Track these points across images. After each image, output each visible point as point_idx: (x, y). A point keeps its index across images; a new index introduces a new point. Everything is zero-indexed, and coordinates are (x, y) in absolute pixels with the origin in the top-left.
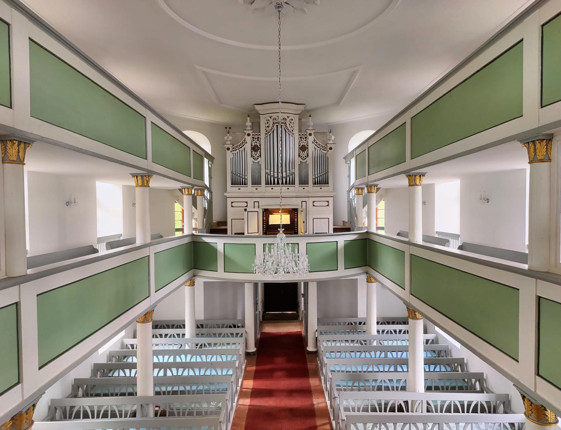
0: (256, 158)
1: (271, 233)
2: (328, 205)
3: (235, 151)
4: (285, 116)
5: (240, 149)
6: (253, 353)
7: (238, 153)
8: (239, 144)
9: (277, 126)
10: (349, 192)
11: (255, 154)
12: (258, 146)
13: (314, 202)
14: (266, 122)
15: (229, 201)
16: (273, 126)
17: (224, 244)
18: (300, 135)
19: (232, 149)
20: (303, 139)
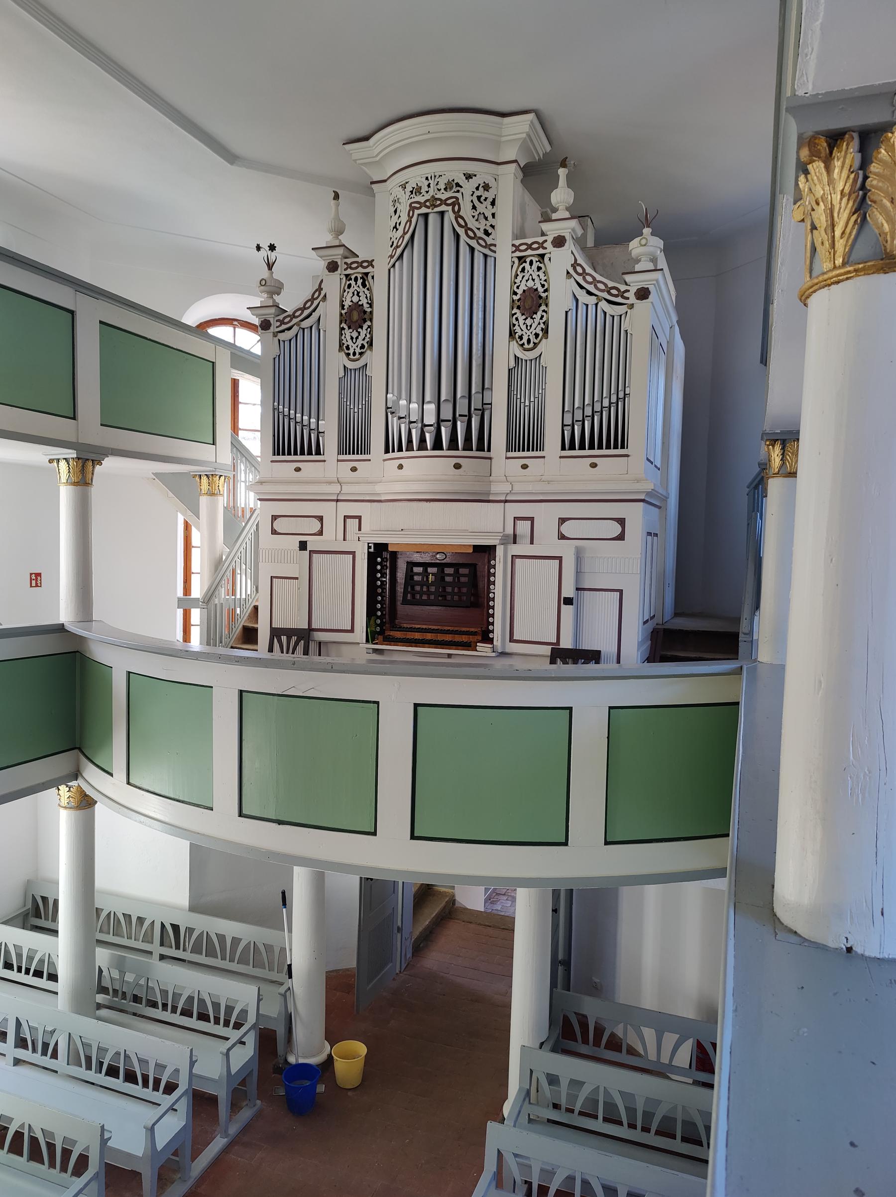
0: (354, 354)
1: (398, 634)
2: (621, 537)
4: (455, 171)
9: (426, 216)
11: (352, 338)
12: (362, 305)
13: (562, 521)
16: (410, 221)
18: (517, 248)
19: (278, 324)
20: (531, 263)
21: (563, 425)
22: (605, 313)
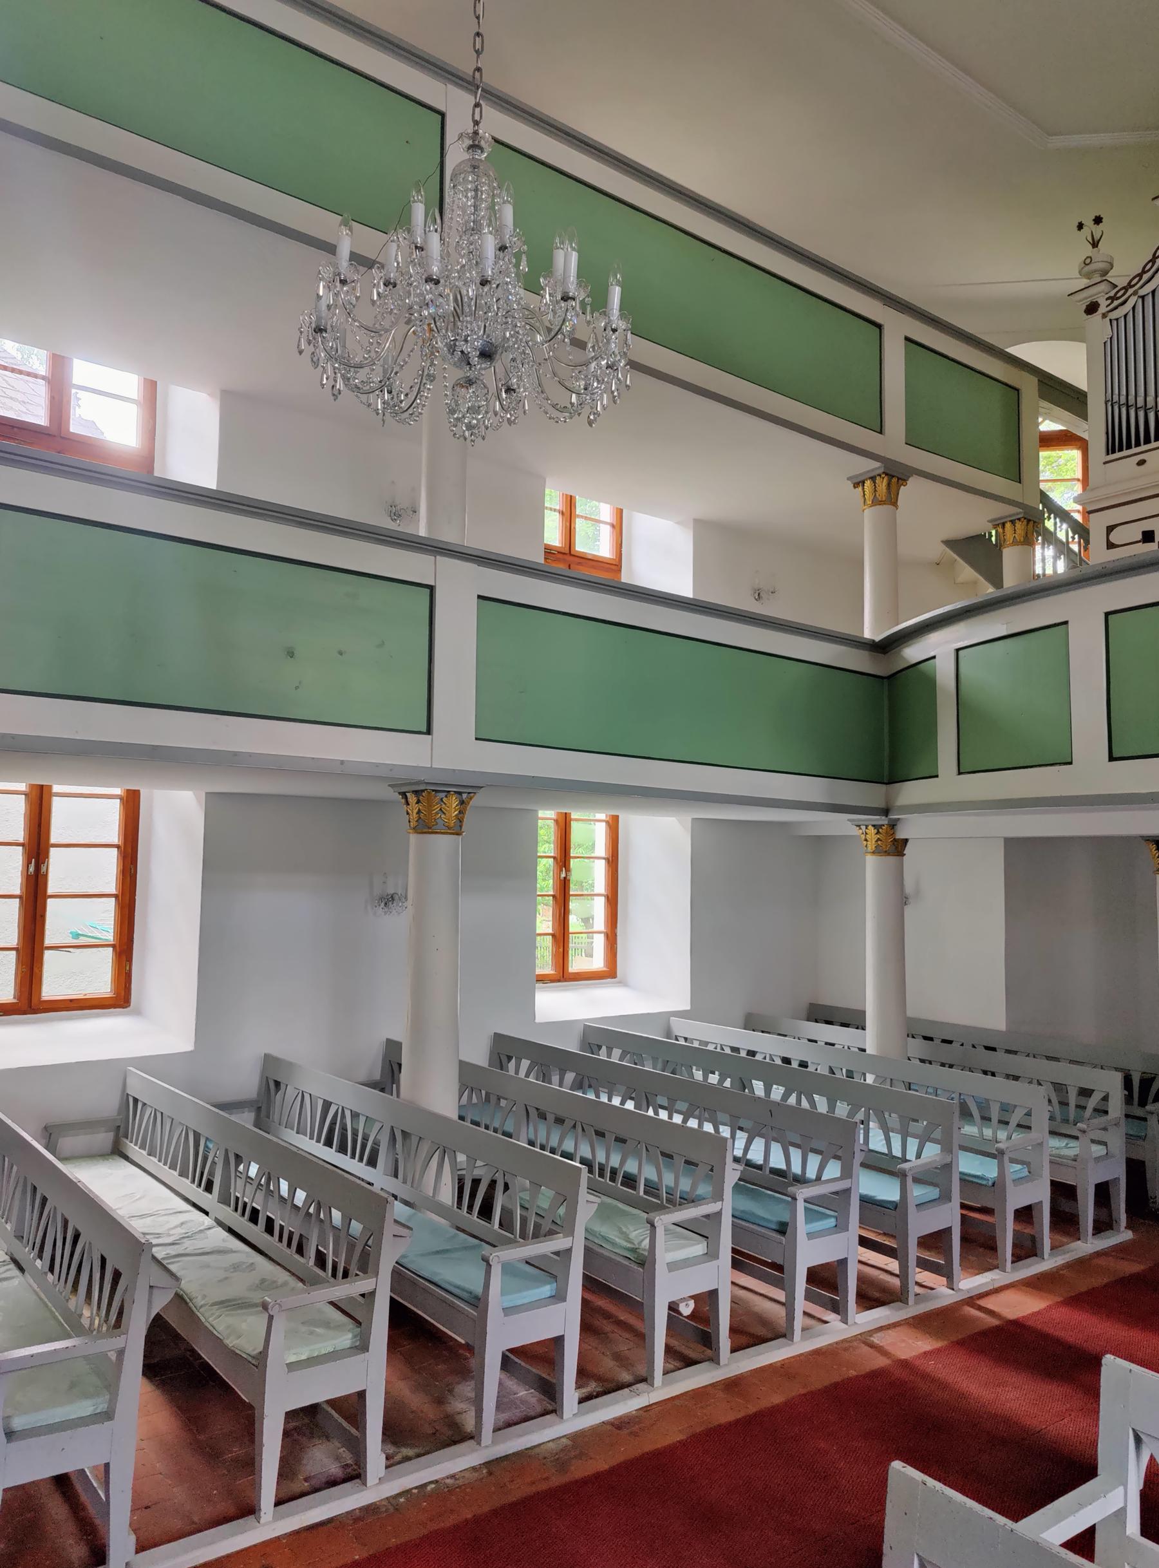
19: (1109, 301)
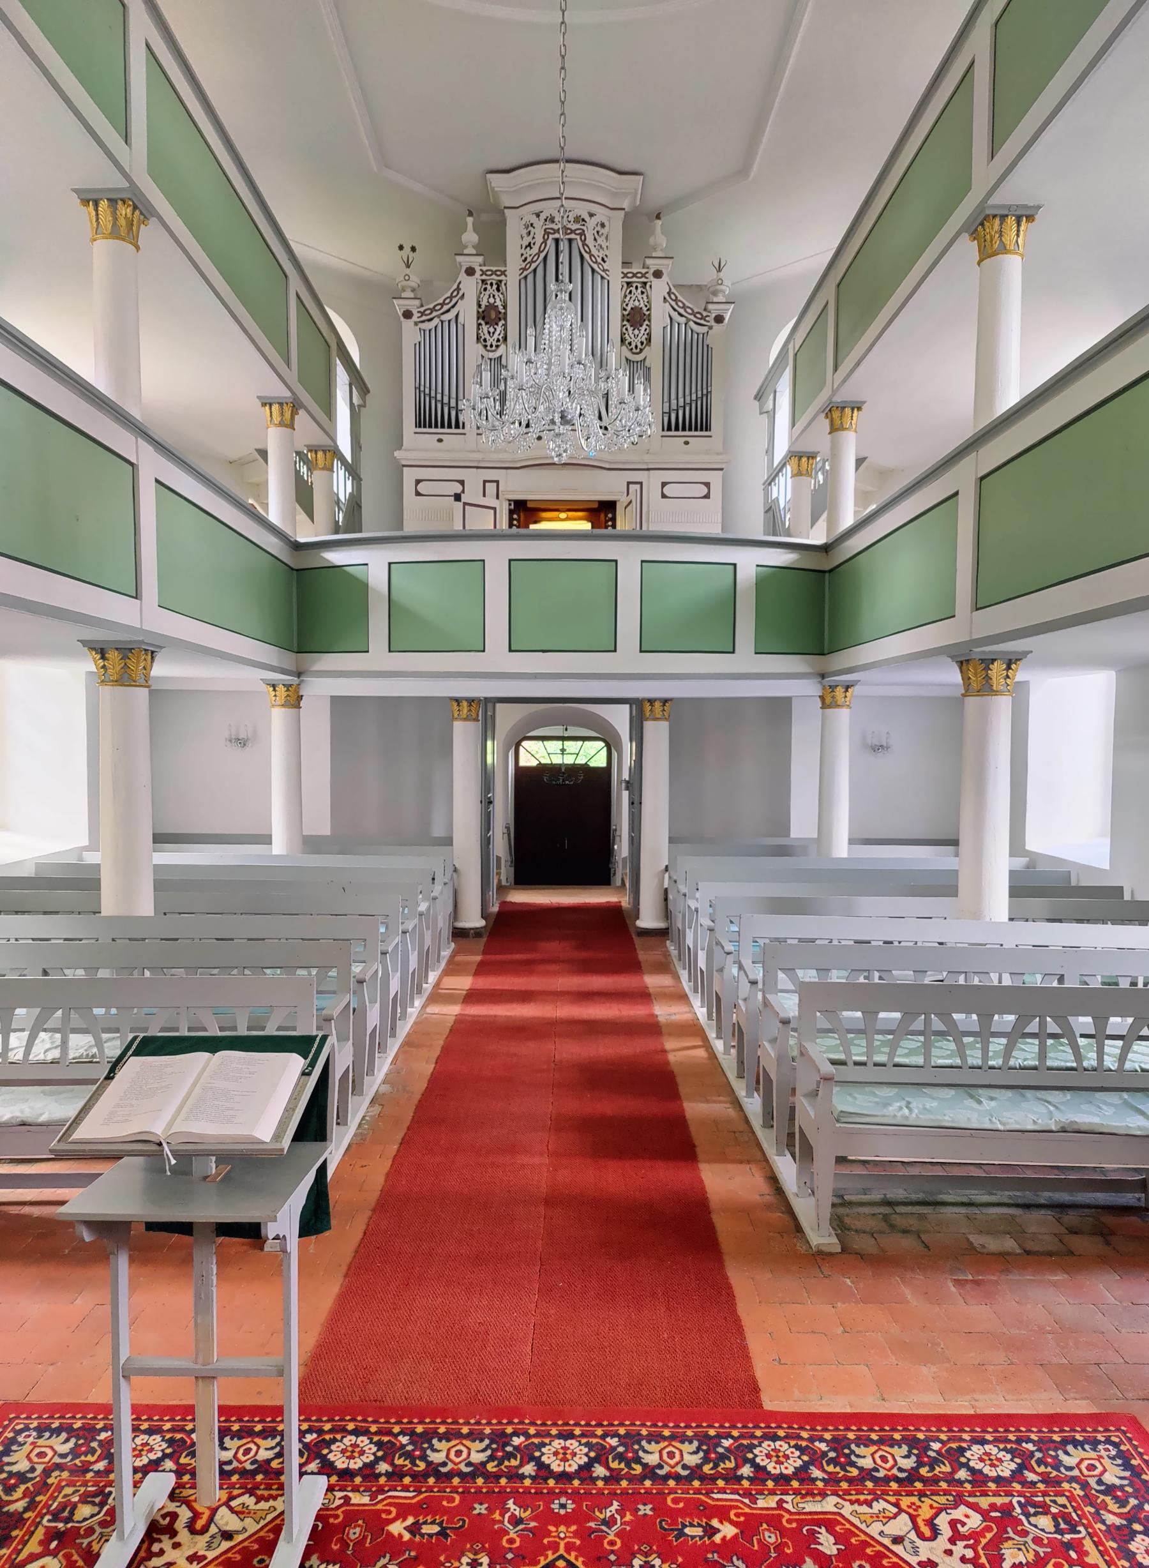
0: (491, 346)
2: (707, 496)
3: (426, 323)
4: (582, 209)
5: (444, 317)
6: (478, 933)
7: (436, 327)
8: (441, 301)
10: (770, 484)
11: (489, 332)
13: (664, 484)
14: (525, 232)
15: (410, 476)
16: (545, 242)
17: (390, 564)
18: (625, 275)
19: (420, 315)
20: (637, 288)
21: (663, 413)
22: (692, 331)
